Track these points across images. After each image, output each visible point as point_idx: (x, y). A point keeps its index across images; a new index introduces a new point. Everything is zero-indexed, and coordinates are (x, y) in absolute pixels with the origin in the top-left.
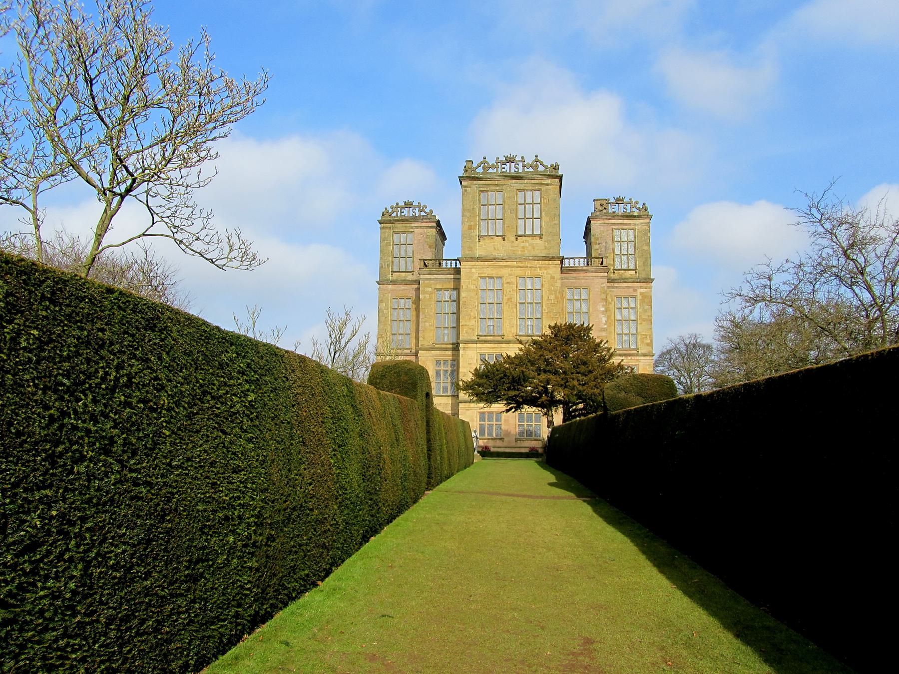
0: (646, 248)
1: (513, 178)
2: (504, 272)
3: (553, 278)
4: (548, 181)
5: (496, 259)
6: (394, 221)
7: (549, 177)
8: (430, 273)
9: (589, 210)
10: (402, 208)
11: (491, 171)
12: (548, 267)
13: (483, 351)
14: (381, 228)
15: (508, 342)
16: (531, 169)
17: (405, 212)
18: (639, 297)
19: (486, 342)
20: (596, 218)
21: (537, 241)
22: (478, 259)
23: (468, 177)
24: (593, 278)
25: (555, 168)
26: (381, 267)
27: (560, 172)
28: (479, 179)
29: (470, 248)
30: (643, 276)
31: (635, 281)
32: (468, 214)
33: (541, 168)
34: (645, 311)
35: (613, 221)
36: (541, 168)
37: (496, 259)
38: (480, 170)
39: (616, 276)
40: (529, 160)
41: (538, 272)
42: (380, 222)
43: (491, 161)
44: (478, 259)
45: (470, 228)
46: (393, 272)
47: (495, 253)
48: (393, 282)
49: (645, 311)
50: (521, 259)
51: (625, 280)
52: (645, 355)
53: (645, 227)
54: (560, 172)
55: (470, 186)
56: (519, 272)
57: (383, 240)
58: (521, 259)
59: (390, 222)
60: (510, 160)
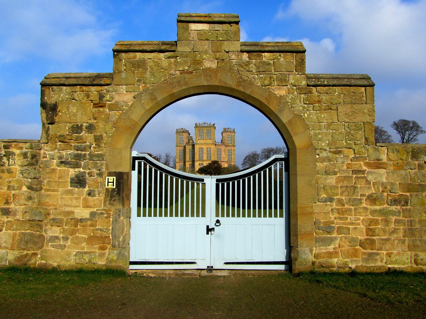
0: (234, 139)
1: (205, 127)
2: (204, 147)
3: (213, 148)
4: (212, 128)
5: (202, 144)
6: (179, 133)
7: (213, 127)
8: (188, 145)
9: (222, 130)
10: (181, 129)
11: (201, 125)
12: (213, 146)
13: (200, 163)
14: (176, 134)
15: (204, 161)
16: (209, 125)
17: (182, 130)
18: (232, 150)
19: (200, 161)
20: (223, 132)
21: (210, 140)
22: (199, 144)
23: (196, 126)
24: (222, 147)
25: (214, 124)
26: (176, 143)
27: (215, 126)
28: (199, 127)
29: (197, 142)
30: (233, 145)
31: (231, 146)
32: (196, 135)
33: (211, 125)
34: (234, 153)
35: (227, 133)
36: (211, 125)
37: (202, 144)
38: (198, 125)
39: (228, 145)
40: (209, 123)
41: (211, 147)
42: (176, 133)
43: (201, 123)
44: (199, 144)
45: (197, 137)
46: (179, 144)
47: (202, 143)
48: (179, 146)
49: (234, 153)
50: (207, 144)
51: (229, 146)
52: (233, 162)
53: (234, 134)
54: (215, 126)
55: (196, 129)
56: (207, 147)
57: (177, 137)
58: (207, 144)
59: (178, 133)
60: (204, 123)
